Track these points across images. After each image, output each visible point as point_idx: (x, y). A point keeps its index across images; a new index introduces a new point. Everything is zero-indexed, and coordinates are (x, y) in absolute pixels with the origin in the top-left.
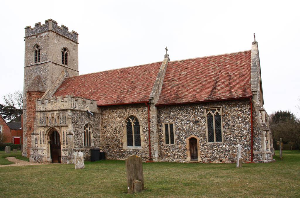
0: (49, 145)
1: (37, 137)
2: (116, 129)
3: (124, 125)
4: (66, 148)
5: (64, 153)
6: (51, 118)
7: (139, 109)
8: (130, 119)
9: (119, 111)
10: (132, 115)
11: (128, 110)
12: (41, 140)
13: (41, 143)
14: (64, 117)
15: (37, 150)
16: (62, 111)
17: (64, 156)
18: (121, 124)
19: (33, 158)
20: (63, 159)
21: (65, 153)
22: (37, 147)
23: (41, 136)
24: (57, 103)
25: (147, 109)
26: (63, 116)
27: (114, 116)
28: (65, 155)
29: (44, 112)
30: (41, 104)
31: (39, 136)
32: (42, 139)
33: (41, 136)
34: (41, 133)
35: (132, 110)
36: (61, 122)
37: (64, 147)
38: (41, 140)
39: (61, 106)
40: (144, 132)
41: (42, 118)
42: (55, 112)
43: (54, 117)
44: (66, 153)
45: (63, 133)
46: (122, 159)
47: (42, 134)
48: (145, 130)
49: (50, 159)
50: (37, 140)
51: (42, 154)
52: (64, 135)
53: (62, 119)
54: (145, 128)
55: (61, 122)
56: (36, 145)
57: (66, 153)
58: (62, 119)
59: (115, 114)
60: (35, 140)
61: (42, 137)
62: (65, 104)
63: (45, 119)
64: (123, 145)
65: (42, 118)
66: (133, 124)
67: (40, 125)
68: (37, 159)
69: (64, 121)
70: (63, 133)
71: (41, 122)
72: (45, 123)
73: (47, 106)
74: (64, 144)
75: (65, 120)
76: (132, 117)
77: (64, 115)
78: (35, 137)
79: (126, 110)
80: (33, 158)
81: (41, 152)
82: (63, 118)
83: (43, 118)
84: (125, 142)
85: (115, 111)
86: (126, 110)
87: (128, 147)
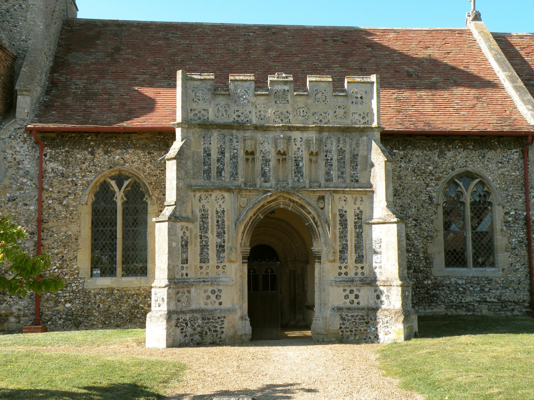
0: (246, 267)
1: (188, 234)
2: (403, 211)
3: (435, 201)
4: (351, 275)
5: (346, 297)
6: (272, 156)
7: (490, 154)
8: (457, 181)
9: (417, 156)
10: (469, 169)
11: (449, 154)
12: (204, 247)
13: (204, 260)
14: (348, 156)
15: (189, 292)
16: (339, 135)
17: (349, 309)
18: (424, 197)
19: (176, 326)
20: (343, 319)
21: (352, 297)
22: (187, 275)
23: (204, 229)
24: (310, 101)
25: (516, 156)
26: (341, 152)
27: (398, 170)
28: (352, 302)
29: (225, 132)
30: (209, 96)
31: (195, 228)
32: (213, 239)
33: (204, 229)
34: (204, 217)
35: (464, 154)
36: (328, 173)
37: (343, 271)
38: (204, 247)
39: (331, 113)
40: (506, 222)
41: (214, 155)
42: (296, 135)
43: (291, 154)
44: (357, 297)
45: (338, 218)
46: (429, 311)
47: (212, 222)
48: (510, 219)
49: (246, 327)
50: (186, 245)
51: (210, 307)
52: (344, 223)
53: (335, 163)
54: (512, 213)
55: (328, 173)
56: (183, 268)
57: (357, 297)
58: (335, 163)
59: (403, 165)
60: (180, 247)
61: (209, 234)
62: (353, 108)
63: (234, 157)
64: (431, 263)
65: (214, 155)
66: (468, 198)
67: (201, 181)
68: (189, 330)
69: (348, 170)
70: (342, 216)
71: (208, 172)
72: (234, 175)
73: (249, 108)
74: (343, 259)
75: (354, 168)
76: (469, 176)
77: (347, 149)
78: (181, 234)
79: (442, 154)
80: (176, 326)
81: (208, 297)
82: (342, 161)
83: (223, 153)
84: (439, 253)
85: (402, 153)
86: (442, 154)
87: (451, 269)
